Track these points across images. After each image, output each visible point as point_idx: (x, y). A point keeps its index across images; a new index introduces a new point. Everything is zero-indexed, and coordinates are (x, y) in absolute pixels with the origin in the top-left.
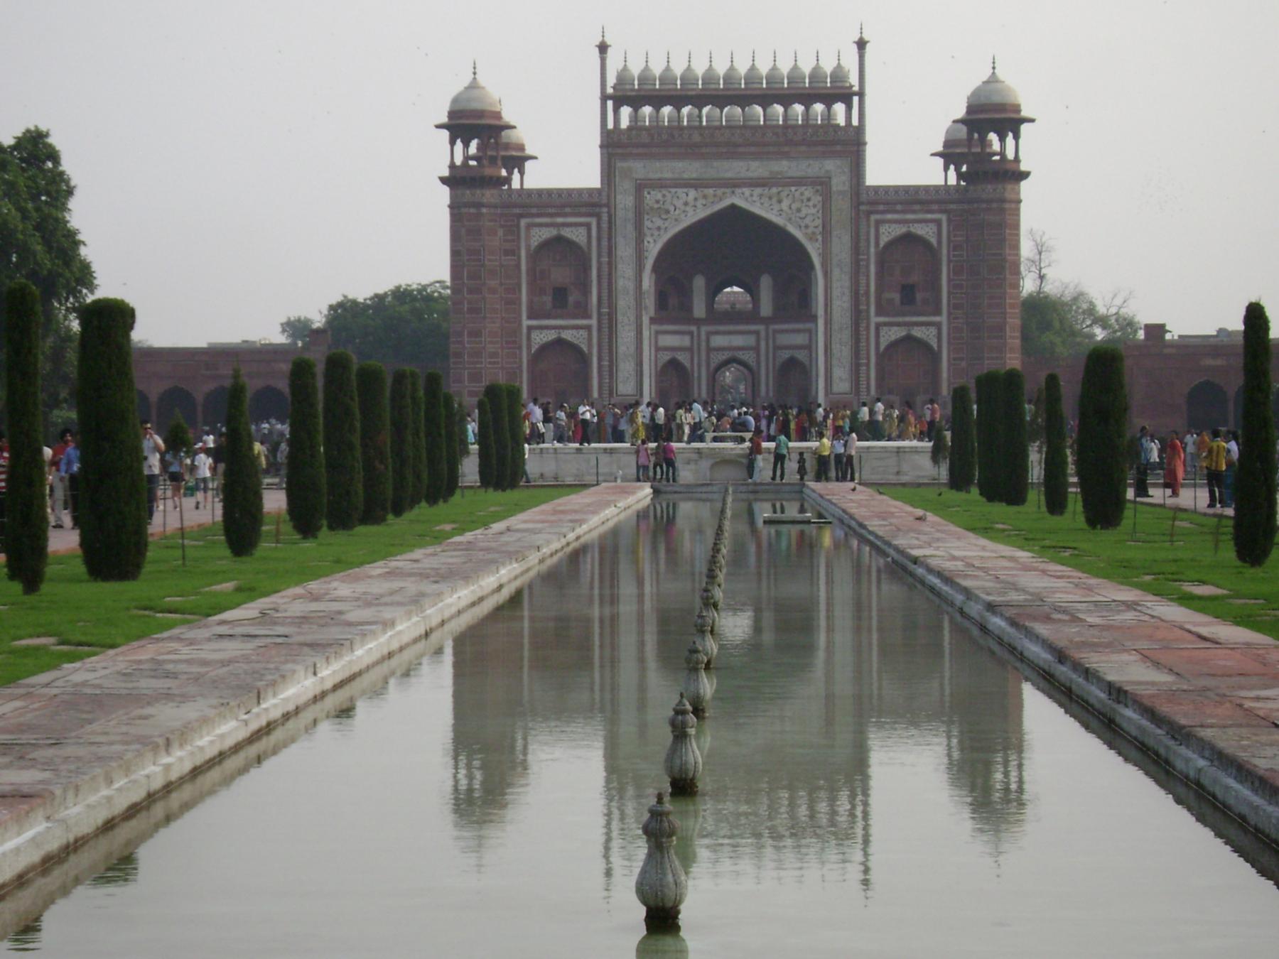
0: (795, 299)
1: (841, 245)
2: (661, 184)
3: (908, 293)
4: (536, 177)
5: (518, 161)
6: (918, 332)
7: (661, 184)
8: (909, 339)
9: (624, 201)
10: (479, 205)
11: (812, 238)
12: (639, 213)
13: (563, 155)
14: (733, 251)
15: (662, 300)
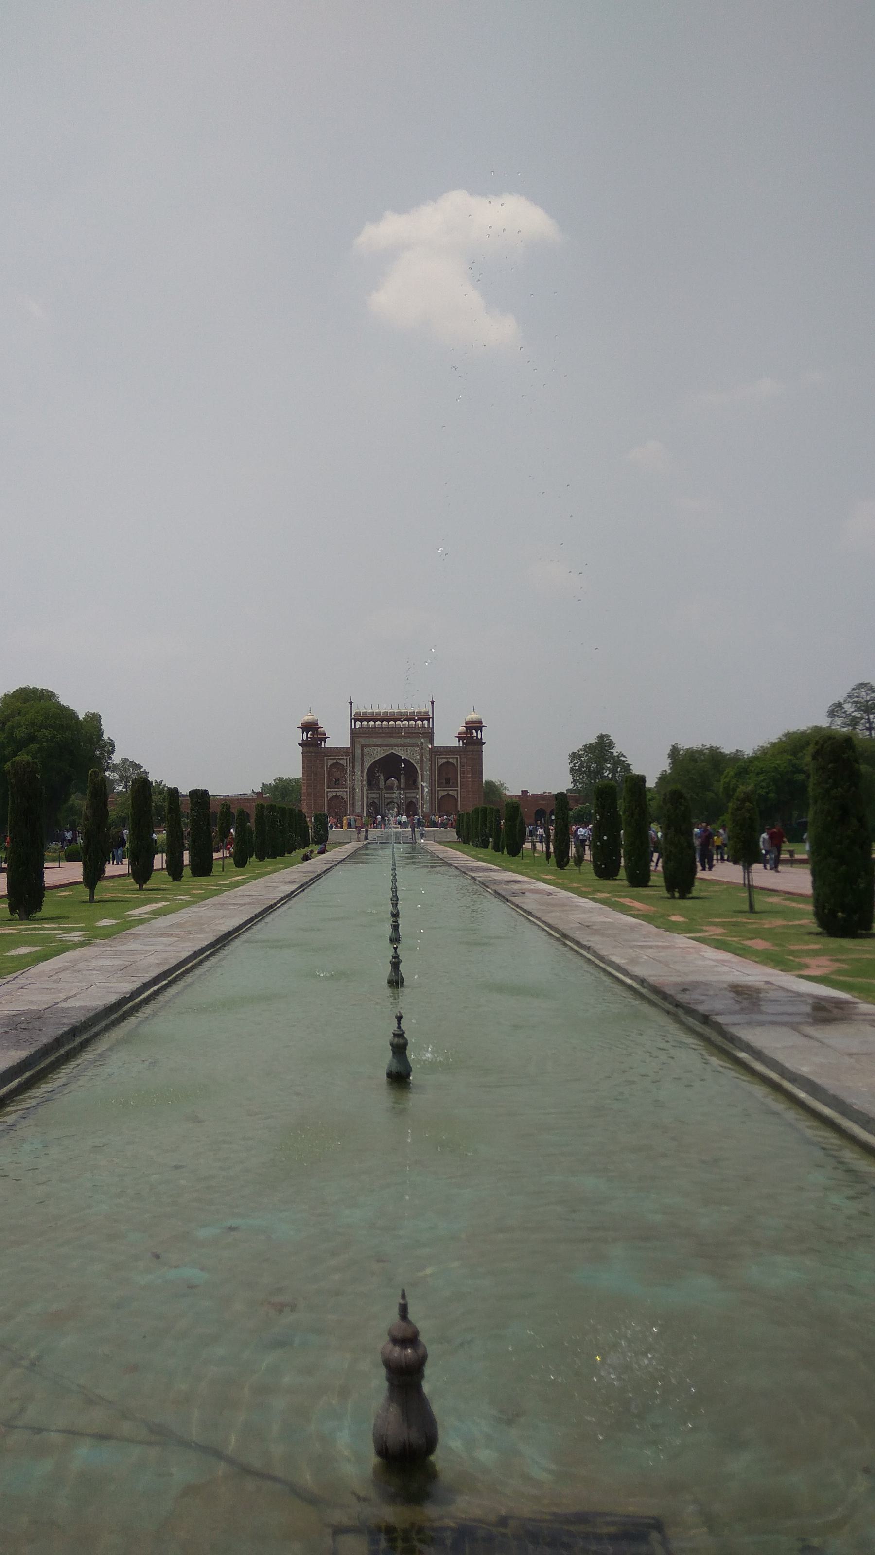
0: (412, 781)
1: (427, 767)
2: (369, 746)
3: (448, 781)
4: (329, 744)
5: (324, 739)
6: (450, 793)
7: (369, 746)
8: (448, 794)
9: (358, 751)
10: (311, 753)
11: (417, 763)
12: (363, 755)
13: (338, 737)
14: (392, 770)
15: (370, 783)
